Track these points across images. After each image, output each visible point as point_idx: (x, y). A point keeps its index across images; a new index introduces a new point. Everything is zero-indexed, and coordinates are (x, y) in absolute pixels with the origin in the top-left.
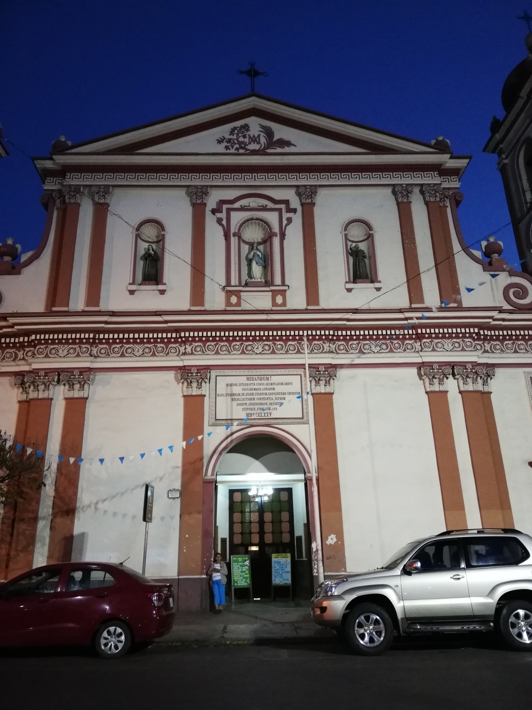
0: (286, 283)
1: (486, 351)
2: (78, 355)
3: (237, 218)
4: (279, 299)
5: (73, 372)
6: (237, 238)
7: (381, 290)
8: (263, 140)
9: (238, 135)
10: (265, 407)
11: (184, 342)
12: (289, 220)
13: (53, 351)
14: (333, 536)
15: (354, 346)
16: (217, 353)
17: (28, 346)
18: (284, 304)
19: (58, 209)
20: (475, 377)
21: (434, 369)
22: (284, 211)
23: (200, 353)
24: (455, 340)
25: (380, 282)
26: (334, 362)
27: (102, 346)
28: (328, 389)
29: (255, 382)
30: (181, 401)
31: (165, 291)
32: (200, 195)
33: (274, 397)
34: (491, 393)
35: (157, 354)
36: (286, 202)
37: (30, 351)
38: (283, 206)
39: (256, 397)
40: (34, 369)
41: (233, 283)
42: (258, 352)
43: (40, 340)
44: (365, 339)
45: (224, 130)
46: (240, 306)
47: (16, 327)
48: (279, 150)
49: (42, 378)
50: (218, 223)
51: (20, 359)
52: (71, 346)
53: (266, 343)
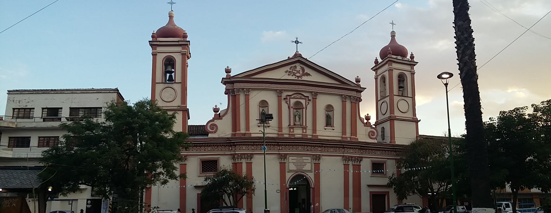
0: (307, 126)
1: (361, 153)
2: (248, 149)
4: (304, 131)
13: (241, 148)
18: (306, 132)
22: (307, 100)
25: (334, 127)
26: (321, 154)
28: (319, 162)
29: (299, 159)
30: (279, 165)
35: (271, 149)
36: (308, 97)
38: (307, 99)
39: (299, 163)
40: (236, 153)
41: (291, 125)
45: (287, 68)
46: (294, 132)
50: (286, 103)
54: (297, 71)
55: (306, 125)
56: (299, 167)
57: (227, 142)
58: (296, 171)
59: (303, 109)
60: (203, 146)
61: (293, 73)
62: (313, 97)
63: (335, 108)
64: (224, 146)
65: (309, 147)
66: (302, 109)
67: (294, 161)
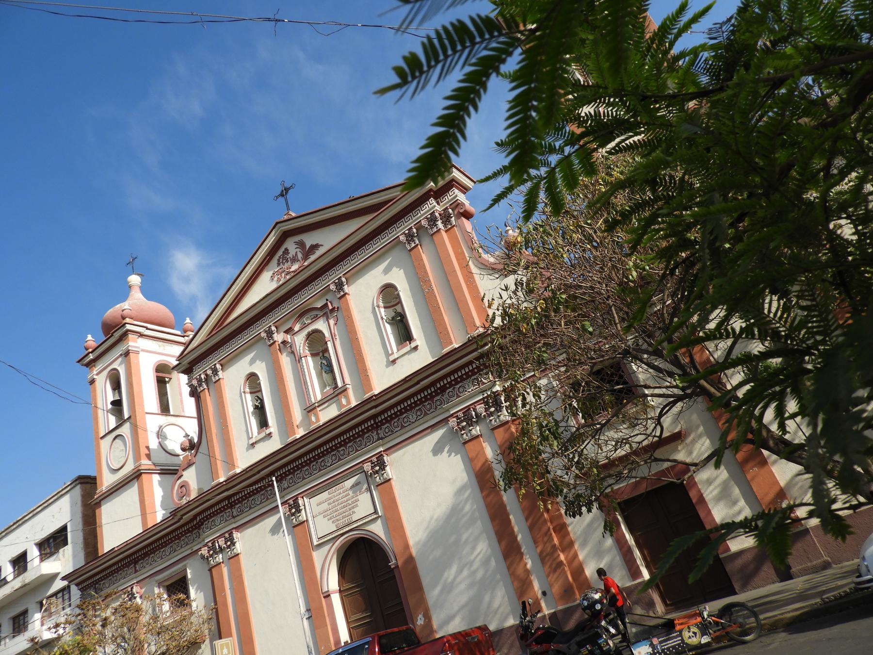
0: (346, 383)
2: (226, 520)
3: (299, 341)
4: (344, 401)
7: (419, 348)
8: (300, 256)
9: (282, 262)
10: (347, 513)
14: (420, 616)
15: (396, 424)
16: (304, 479)
18: (349, 402)
20: (498, 409)
21: (460, 418)
23: (293, 484)
24: (473, 378)
31: (270, 433)
32: (269, 335)
33: (350, 502)
35: (269, 497)
42: (329, 465)
43: (202, 518)
44: (402, 414)
45: (273, 267)
47: (184, 517)
53: (332, 453)
55: (344, 382)
56: (343, 517)
57: (181, 521)
58: (339, 533)
60: (157, 550)
62: (339, 296)
63: (399, 289)
64: (188, 531)
65: (348, 446)
67: (325, 506)
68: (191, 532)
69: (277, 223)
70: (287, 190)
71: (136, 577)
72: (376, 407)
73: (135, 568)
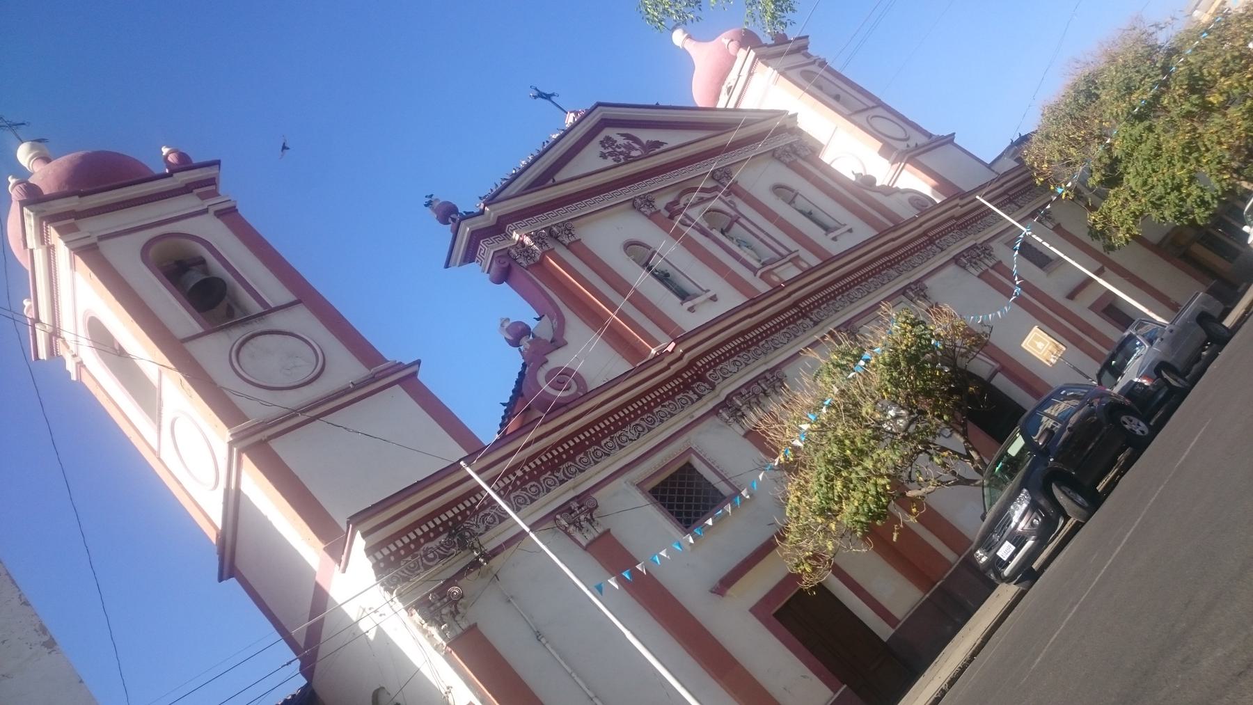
0: (793, 250)
2: (747, 365)
3: (696, 214)
5: (765, 378)
6: (714, 230)
8: (637, 146)
11: (805, 316)
12: (734, 204)
17: (694, 381)
19: (527, 269)
27: (752, 349)
34: (1000, 262)
37: (698, 386)
47: (686, 356)
48: (657, 150)
49: (747, 396)
51: (697, 400)
52: (731, 360)
53: (856, 287)
54: (624, 147)
57: (673, 367)
59: (737, 221)
60: (605, 437)
61: (621, 153)
64: (669, 396)
65: (870, 280)
66: (736, 225)
68: (672, 398)
69: (599, 104)
70: (548, 97)
71: (574, 488)
72: (893, 240)
73: (557, 477)
